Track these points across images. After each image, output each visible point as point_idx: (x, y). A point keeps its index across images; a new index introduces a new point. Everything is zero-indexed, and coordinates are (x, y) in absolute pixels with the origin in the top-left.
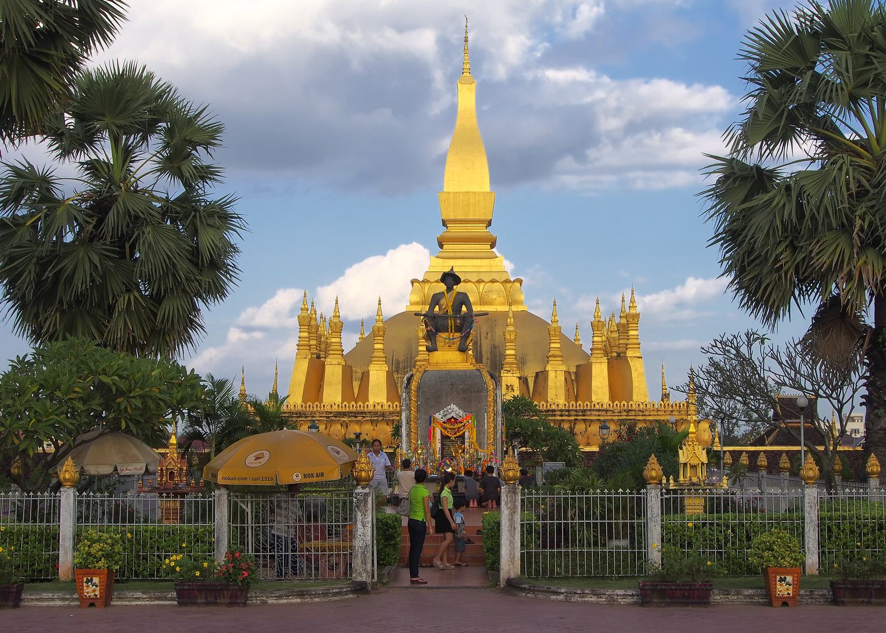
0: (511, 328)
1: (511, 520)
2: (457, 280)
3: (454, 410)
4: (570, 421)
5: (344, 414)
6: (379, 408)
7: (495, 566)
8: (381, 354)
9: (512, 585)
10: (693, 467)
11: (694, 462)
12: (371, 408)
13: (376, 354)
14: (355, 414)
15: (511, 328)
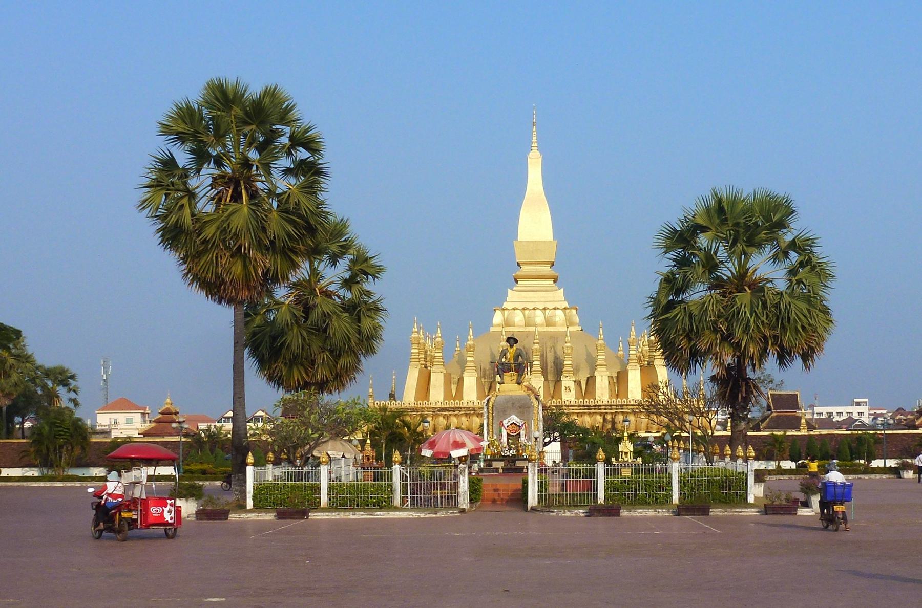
0: (568, 345)
1: (533, 479)
2: (516, 341)
3: (514, 419)
4: (612, 413)
5: (445, 409)
6: (471, 405)
7: (526, 501)
8: (473, 365)
9: (533, 509)
10: (626, 453)
11: (626, 450)
12: (465, 405)
13: (468, 365)
14: (454, 409)
15: (568, 345)
